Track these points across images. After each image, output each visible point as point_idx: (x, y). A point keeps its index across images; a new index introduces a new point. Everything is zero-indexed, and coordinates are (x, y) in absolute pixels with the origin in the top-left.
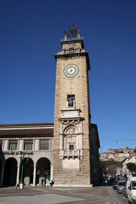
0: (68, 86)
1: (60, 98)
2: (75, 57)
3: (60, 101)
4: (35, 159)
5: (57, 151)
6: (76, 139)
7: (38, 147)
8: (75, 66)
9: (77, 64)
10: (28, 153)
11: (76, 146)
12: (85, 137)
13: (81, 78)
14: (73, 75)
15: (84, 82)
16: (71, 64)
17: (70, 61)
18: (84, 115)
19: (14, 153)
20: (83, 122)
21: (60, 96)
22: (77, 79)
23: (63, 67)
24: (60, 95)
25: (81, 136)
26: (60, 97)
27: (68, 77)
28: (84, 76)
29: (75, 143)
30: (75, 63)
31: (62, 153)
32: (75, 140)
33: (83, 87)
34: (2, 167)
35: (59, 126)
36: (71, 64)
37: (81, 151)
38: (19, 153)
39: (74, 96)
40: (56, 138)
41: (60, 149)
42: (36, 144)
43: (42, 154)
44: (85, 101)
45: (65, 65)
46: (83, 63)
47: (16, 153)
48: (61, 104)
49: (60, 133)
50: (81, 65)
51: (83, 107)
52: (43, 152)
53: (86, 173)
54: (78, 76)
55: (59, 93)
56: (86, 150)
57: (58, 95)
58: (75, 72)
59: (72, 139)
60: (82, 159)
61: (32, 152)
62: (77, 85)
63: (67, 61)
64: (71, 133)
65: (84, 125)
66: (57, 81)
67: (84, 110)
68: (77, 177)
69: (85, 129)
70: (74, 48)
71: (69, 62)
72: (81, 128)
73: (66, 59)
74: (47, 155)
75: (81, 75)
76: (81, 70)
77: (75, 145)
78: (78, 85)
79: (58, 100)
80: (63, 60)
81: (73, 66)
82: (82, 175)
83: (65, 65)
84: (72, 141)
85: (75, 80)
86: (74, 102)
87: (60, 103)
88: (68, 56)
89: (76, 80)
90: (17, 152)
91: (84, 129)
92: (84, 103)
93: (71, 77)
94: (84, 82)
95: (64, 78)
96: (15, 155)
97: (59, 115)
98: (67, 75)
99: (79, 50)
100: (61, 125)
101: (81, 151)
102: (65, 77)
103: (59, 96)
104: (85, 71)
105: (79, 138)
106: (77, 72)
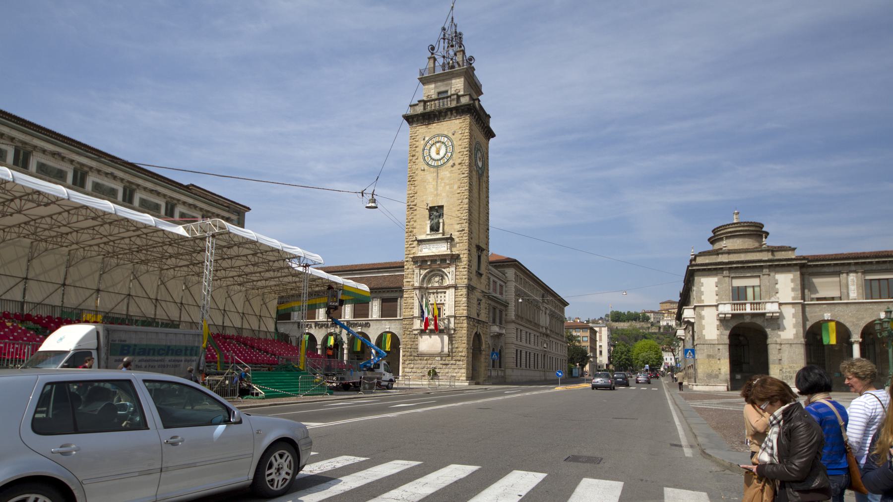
0: (430, 188)
1: (415, 215)
3: (415, 221)
5: (410, 320)
6: (445, 297)
7: (378, 312)
8: (446, 139)
9: (450, 135)
10: (361, 323)
11: (445, 310)
12: (460, 293)
13: (457, 167)
14: (442, 161)
16: (439, 135)
17: (437, 128)
18: (461, 249)
21: (416, 210)
22: (450, 170)
23: (422, 142)
24: (415, 208)
25: (452, 291)
26: (415, 213)
28: (463, 162)
30: (446, 133)
32: (443, 299)
33: (461, 189)
35: (414, 271)
36: (439, 135)
37: (452, 320)
39: (442, 207)
42: (374, 307)
43: (385, 325)
44: (464, 218)
45: (427, 139)
46: (463, 132)
48: (418, 227)
49: (415, 286)
50: (458, 136)
51: (459, 231)
52: (387, 322)
53: (460, 361)
54: (451, 162)
56: (462, 318)
57: (411, 208)
58: (445, 154)
59: (437, 297)
61: (366, 322)
62: (448, 185)
63: (430, 128)
64: (436, 285)
65: (459, 268)
66: (411, 176)
67: (461, 238)
68: (444, 367)
70: (447, 92)
71: (434, 129)
72: (452, 275)
74: (393, 327)
75: (459, 161)
76: (457, 149)
77: (444, 308)
78: (451, 184)
79: (412, 218)
80: (422, 127)
81: (442, 140)
82: (451, 364)
83: (427, 139)
85: (445, 173)
86: (441, 221)
87: (415, 224)
88: (432, 116)
89: (448, 172)
91: (458, 277)
92: (461, 222)
93: (438, 166)
95: (423, 169)
97: (414, 250)
98: (430, 163)
99: (453, 100)
100: (417, 271)
101: (452, 320)
102: (426, 167)
103: (413, 210)
104: (467, 149)
106: (450, 154)
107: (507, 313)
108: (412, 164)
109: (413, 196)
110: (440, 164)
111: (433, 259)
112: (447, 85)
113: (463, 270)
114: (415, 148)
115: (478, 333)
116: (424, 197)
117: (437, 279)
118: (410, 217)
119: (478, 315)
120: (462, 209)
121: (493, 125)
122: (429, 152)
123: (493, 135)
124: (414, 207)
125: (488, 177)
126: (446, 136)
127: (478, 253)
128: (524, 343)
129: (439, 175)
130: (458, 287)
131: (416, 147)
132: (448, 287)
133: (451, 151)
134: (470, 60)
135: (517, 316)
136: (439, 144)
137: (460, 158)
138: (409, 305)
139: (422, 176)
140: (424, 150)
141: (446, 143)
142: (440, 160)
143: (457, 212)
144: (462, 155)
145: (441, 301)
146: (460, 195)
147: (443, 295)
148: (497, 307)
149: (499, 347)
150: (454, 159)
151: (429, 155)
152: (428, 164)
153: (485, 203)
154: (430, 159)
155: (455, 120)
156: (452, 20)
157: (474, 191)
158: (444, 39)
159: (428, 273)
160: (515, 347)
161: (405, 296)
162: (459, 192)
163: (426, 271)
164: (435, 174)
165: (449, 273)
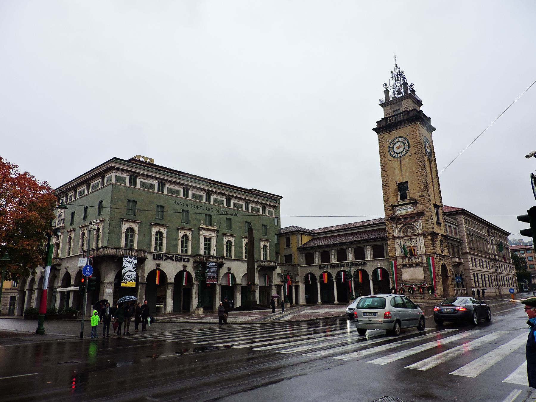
2: (402, 127)
3: (389, 194)
4: (369, 269)
6: (417, 241)
9: (405, 136)
11: (418, 250)
14: (402, 153)
15: (419, 161)
16: (398, 138)
17: (395, 133)
19: (344, 264)
20: (423, 219)
21: (389, 186)
22: (409, 158)
27: (395, 157)
28: (417, 152)
29: (416, 246)
30: (402, 135)
31: (400, 261)
34: (333, 282)
35: (392, 226)
36: (398, 138)
38: (350, 264)
40: (391, 243)
41: (397, 256)
42: (368, 251)
47: (346, 264)
52: (378, 262)
54: (409, 153)
55: (386, 182)
57: (385, 185)
59: (411, 242)
60: (427, 266)
67: (423, 202)
69: (427, 227)
73: (390, 131)
75: (415, 152)
76: (412, 144)
80: (386, 134)
81: (401, 140)
83: (390, 141)
84: (412, 244)
90: (348, 263)
93: (400, 157)
94: (419, 161)
96: (346, 267)
98: (394, 155)
100: (394, 226)
101: (424, 257)
102: (392, 158)
105: (420, 239)
106: (407, 148)
107: (462, 247)
108: (383, 158)
109: (386, 178)
110: (401, 155)
111: (406, 217)
112: (399, 105)
113: (427, 222)
114: (383, 148)
115: (444, 265)
116: (393, 177)
117: (409, 230)
118: (386, 191)
119: (442, 252)
120: (421, 182)
121: (433, 123)
122: (393, 149)
123: (434, 129)
124: (387, 184)
125: (435, 157)
126: (403, 137)
127: (436, 210)
128: (478, 268)
129: (402, 162)
130: (426, 234)
131: (383, 147)
132: (418, 235)
133: (408, 146)
134: (411, 86)
135: (470, 248)
136: (399, 143)
137: (414, 150)
138: (392, 249)
139: (390, 165)
140: (389, 148)
141: (404, 142)
142: (401, 153)
143: (417, 185)
144: (416, 148)
145: (414, 244)
146: (418, 173)
147: (415, 240)
148: (454, 244)
149: (460, 272)
150: (410, 151)
151: (393, 150)
152: (393, 156)
153: (435, 174)
154: (394, 153)
155: (408, 127)
156: (396, 65)
157: (427, 169)
158: (393, 77)
159: (403, 226)
160: (472, 272)
161: (388, 243)
162: (417, 171)
163: (401, 225)
164: (399, 162)
165: (418, 225)
